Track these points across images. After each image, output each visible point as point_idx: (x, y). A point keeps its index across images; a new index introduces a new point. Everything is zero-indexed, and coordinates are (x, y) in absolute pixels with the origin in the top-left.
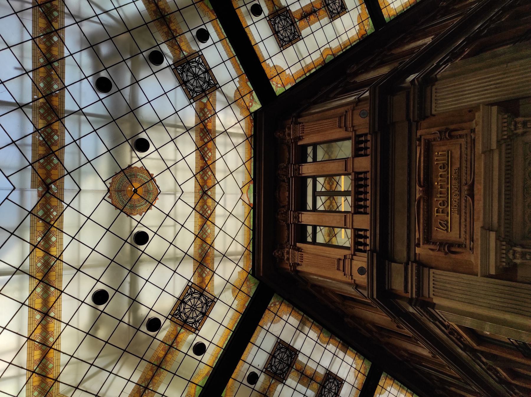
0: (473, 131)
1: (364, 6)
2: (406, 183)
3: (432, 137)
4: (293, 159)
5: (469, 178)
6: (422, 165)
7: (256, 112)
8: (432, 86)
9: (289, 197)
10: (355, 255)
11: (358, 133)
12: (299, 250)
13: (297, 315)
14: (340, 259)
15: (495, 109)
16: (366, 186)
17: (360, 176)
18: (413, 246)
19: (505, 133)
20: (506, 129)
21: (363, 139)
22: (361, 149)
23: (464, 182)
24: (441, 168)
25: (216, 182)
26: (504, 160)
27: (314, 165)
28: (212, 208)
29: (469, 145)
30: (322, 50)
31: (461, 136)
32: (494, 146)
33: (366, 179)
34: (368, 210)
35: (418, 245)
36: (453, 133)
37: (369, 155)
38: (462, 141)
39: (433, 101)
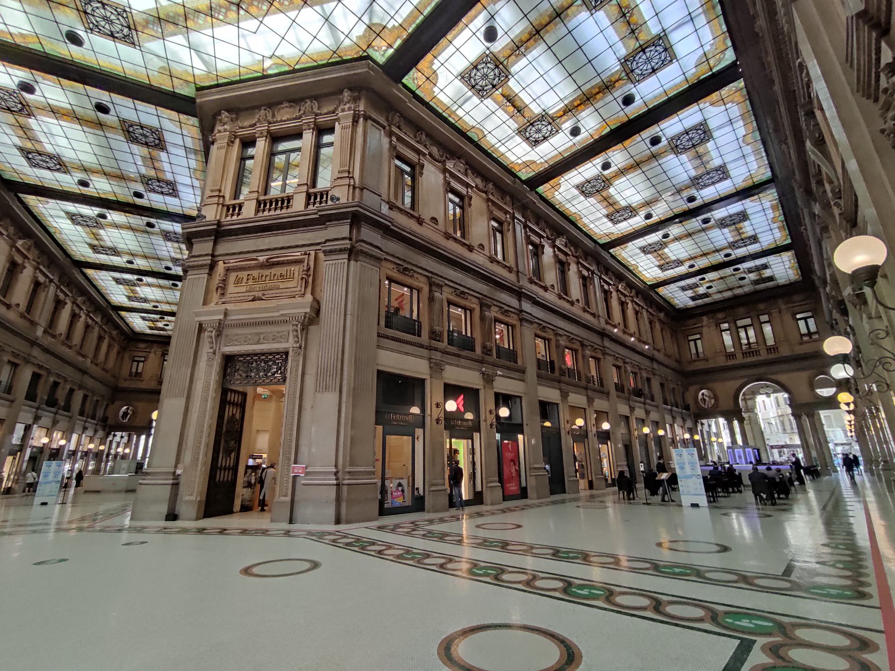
1: (546, 166)
4: (321, 119)
7: (368, 57)
9: (282, 121)
10: (223, 206)
12: (231, 143)
13: (198, 144)
14: (220, 191)
18: (226, 258)
23: (265, 293)
25: (261, 19)
26: (277, 319)
28: (227, 20)
30: (478, 126)
32: (281, 312)
34: (260, 214)
35: (225, 263)
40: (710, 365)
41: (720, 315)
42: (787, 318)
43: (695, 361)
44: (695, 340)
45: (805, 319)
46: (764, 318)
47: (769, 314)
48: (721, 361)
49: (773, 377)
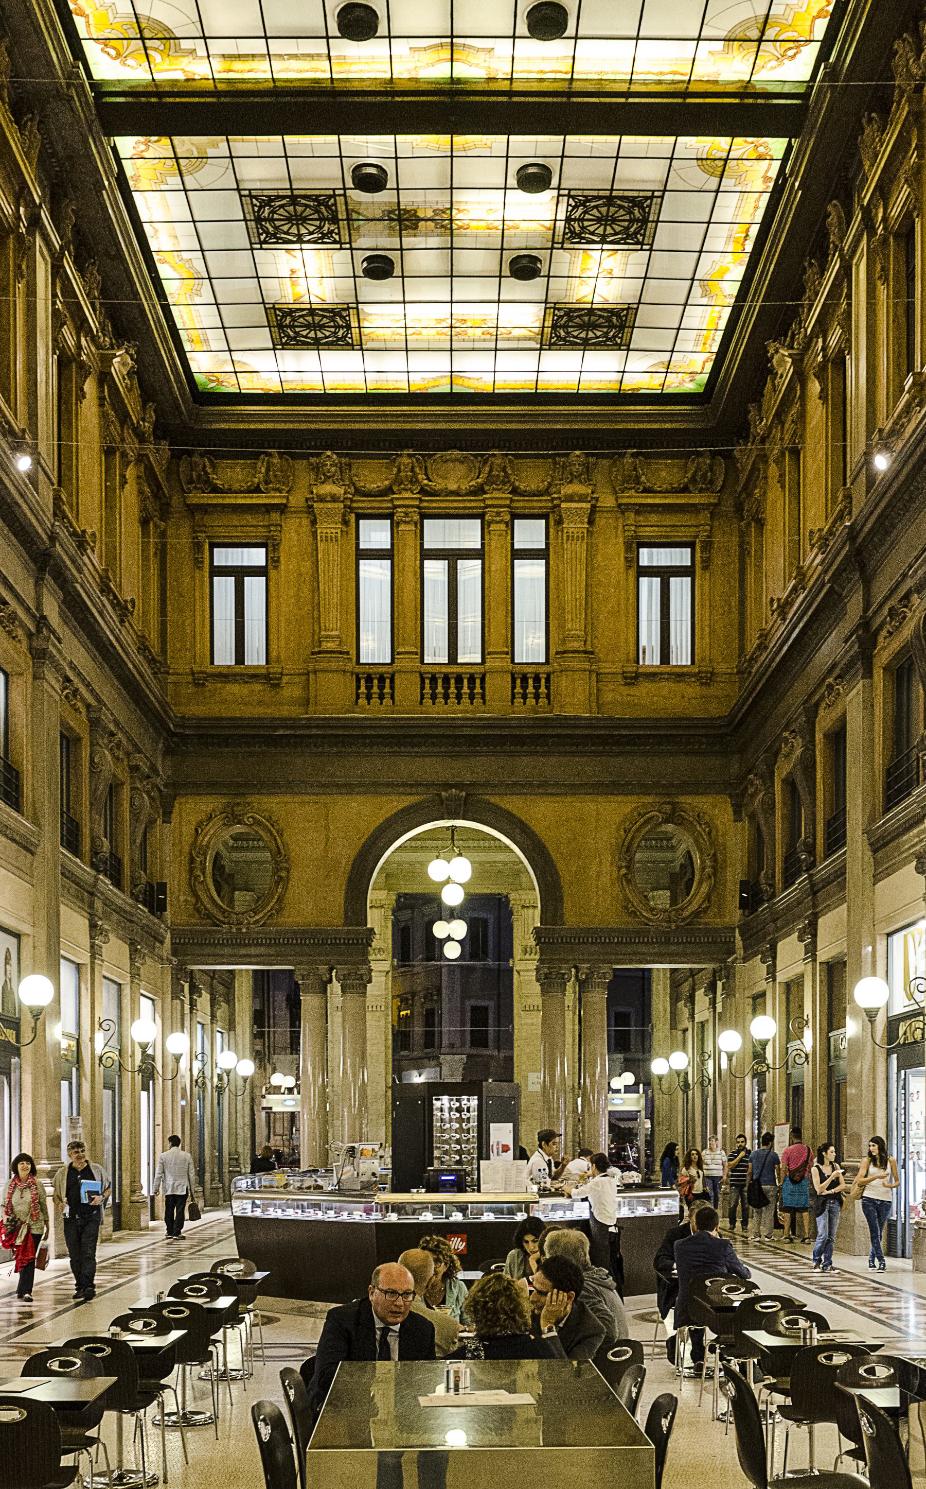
41: (373, 476)
42: (612, 549)
43: (224, 676)
45: (665, 574)
46: (529, 533)
47: (551, 517)
48: (334, 697)
49: (512, 804)
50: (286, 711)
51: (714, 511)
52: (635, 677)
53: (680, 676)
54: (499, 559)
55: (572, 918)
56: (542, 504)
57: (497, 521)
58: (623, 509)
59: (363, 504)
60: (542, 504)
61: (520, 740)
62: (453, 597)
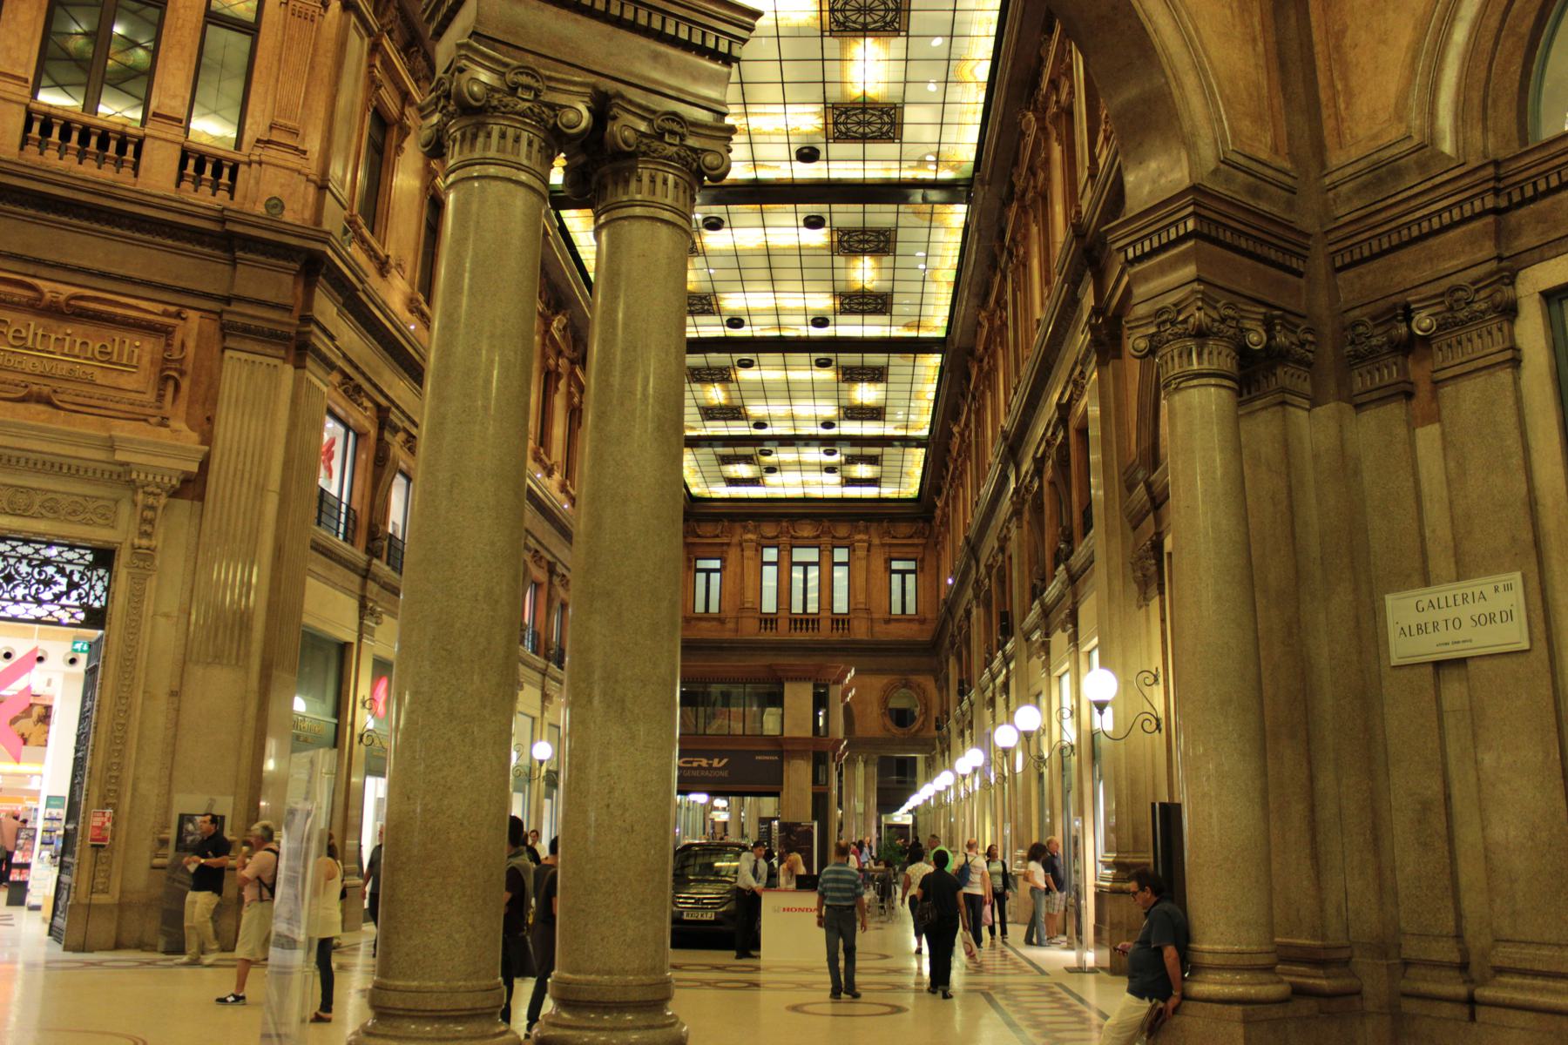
0: (163, 422)
2: (85, 263)
3: (177, 343)
5: (67, 398)
6: (119, 311)
8: (284, 360)
11: (242, 168)
15: (194, 468)
16: (101, 160)
17: (131, 148)
19: (142, 476)
20: (150, 477)
21: (225, 179)
22: (200, 169)
24: (104, 346)
27: (195, 16)
29: (138, 410)
31: (160, 397)
32: (120, 456)
33: (119, 164)
36: (171, 384)
37: (178, 186)
38: (150, 397)
39: (251, 357)
40: (727, 634)
41: (769, 530)
42: (878, 563)
43: (700, 618)
44: (708, 571)
45: (903, 573)
46: (841, 555)
47: (851, 548)
48: (750, 630)
50: (727, 635)
51: (925, 546)
52: (889, 621)
53: (910, 620)
54: (826, 566)
55: (859, 732)
56: (846, 542)
57: (826, 551)
58: (883, 545)
59: (765, 542)
60: (846, 542)
61: (834, 650)
62: (808, 584)
